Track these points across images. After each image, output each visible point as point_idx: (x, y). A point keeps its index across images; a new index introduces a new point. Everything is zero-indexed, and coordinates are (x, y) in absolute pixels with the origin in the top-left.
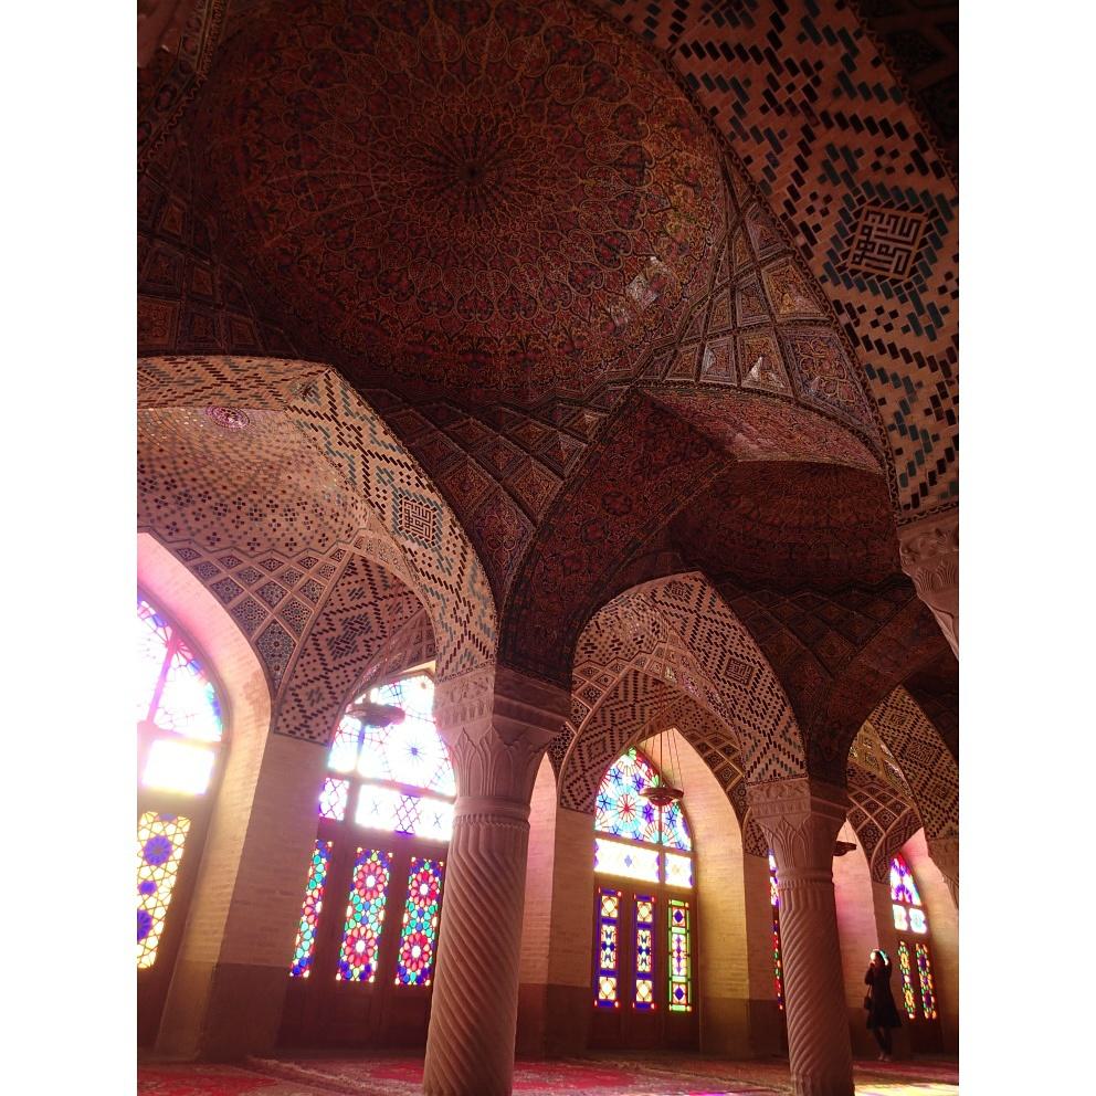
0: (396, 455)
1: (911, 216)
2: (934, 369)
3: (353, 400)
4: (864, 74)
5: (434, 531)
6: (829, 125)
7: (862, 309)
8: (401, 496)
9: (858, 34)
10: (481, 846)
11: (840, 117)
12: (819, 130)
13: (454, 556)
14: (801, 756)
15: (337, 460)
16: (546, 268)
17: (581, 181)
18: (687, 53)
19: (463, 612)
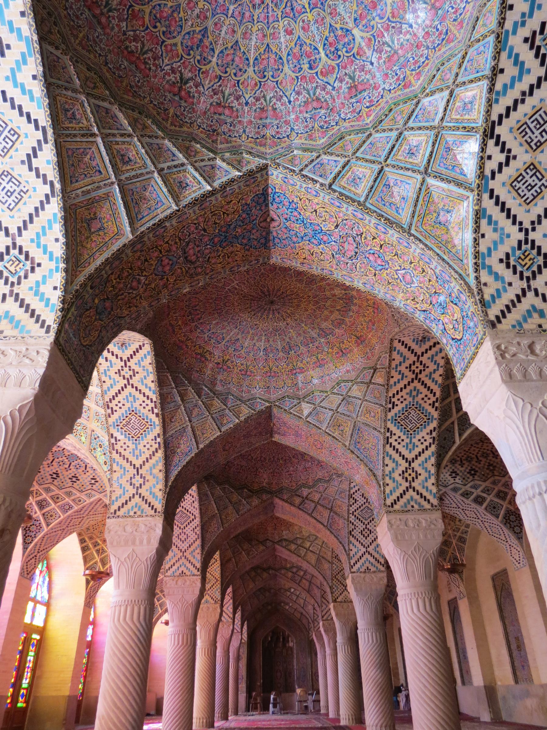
0: (147, 392)
1: (423, 416)
2: (406, 462)
3: (150, 359)
4: (436, 376)
5: (142, 434)
6: (419, 382)
7: (395, 434)
8: (133, 411)
9: (442, 367)
10: (142, 618)
11: (423, 382)
12: (416, 382)
13: (146, 451)
14: (198, 565)
15: (104, 378)
16: (259, 340)
17: (303, 325)
18: (399, 341)
19: (138, 481)
